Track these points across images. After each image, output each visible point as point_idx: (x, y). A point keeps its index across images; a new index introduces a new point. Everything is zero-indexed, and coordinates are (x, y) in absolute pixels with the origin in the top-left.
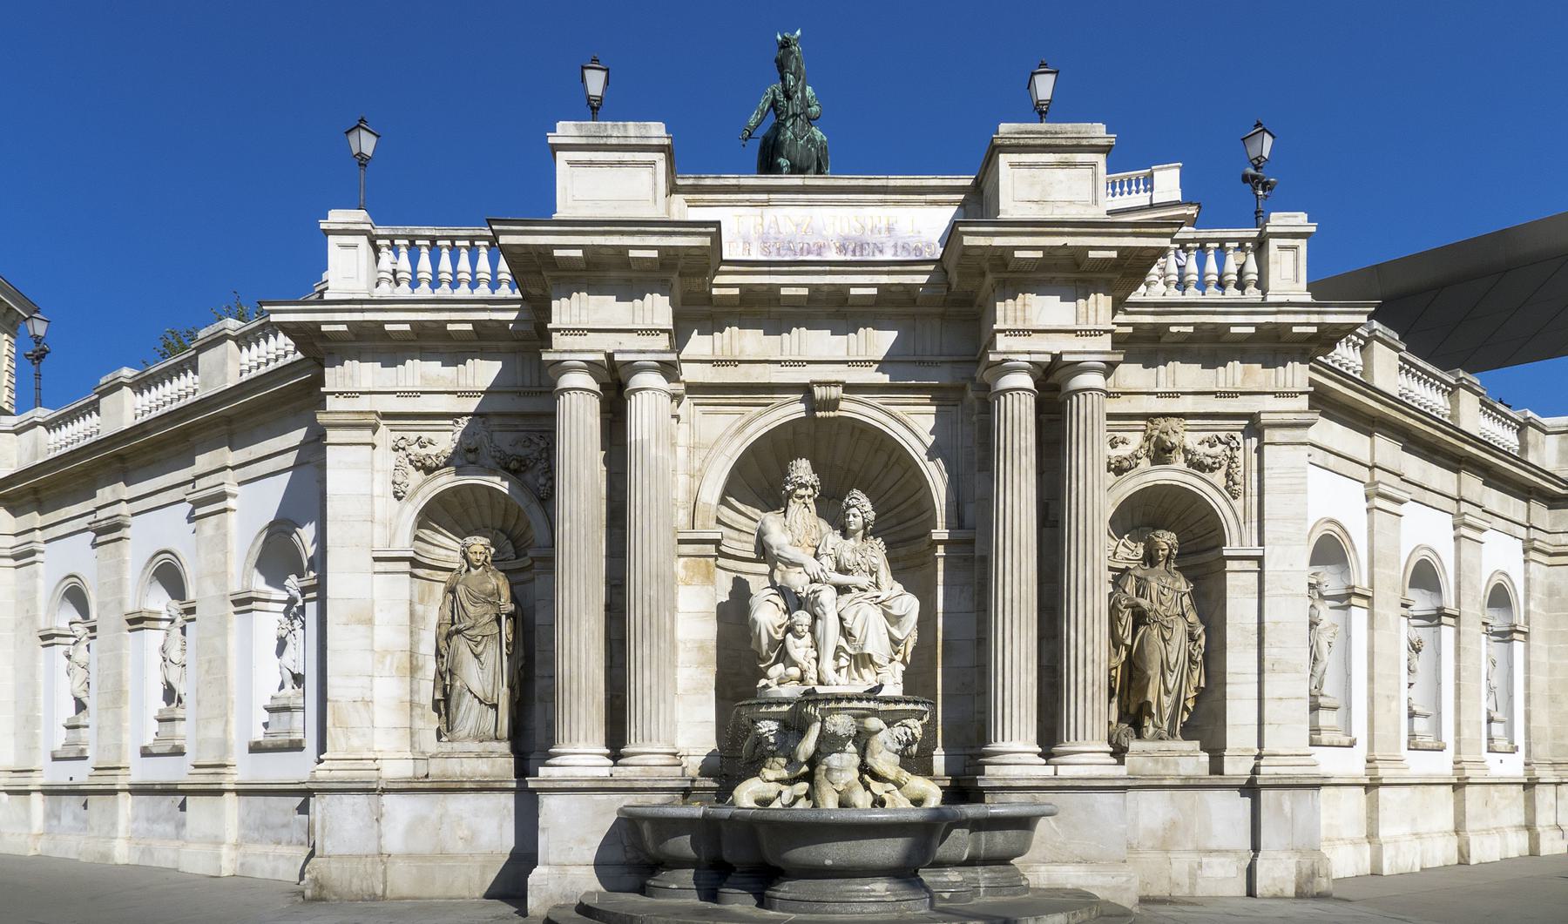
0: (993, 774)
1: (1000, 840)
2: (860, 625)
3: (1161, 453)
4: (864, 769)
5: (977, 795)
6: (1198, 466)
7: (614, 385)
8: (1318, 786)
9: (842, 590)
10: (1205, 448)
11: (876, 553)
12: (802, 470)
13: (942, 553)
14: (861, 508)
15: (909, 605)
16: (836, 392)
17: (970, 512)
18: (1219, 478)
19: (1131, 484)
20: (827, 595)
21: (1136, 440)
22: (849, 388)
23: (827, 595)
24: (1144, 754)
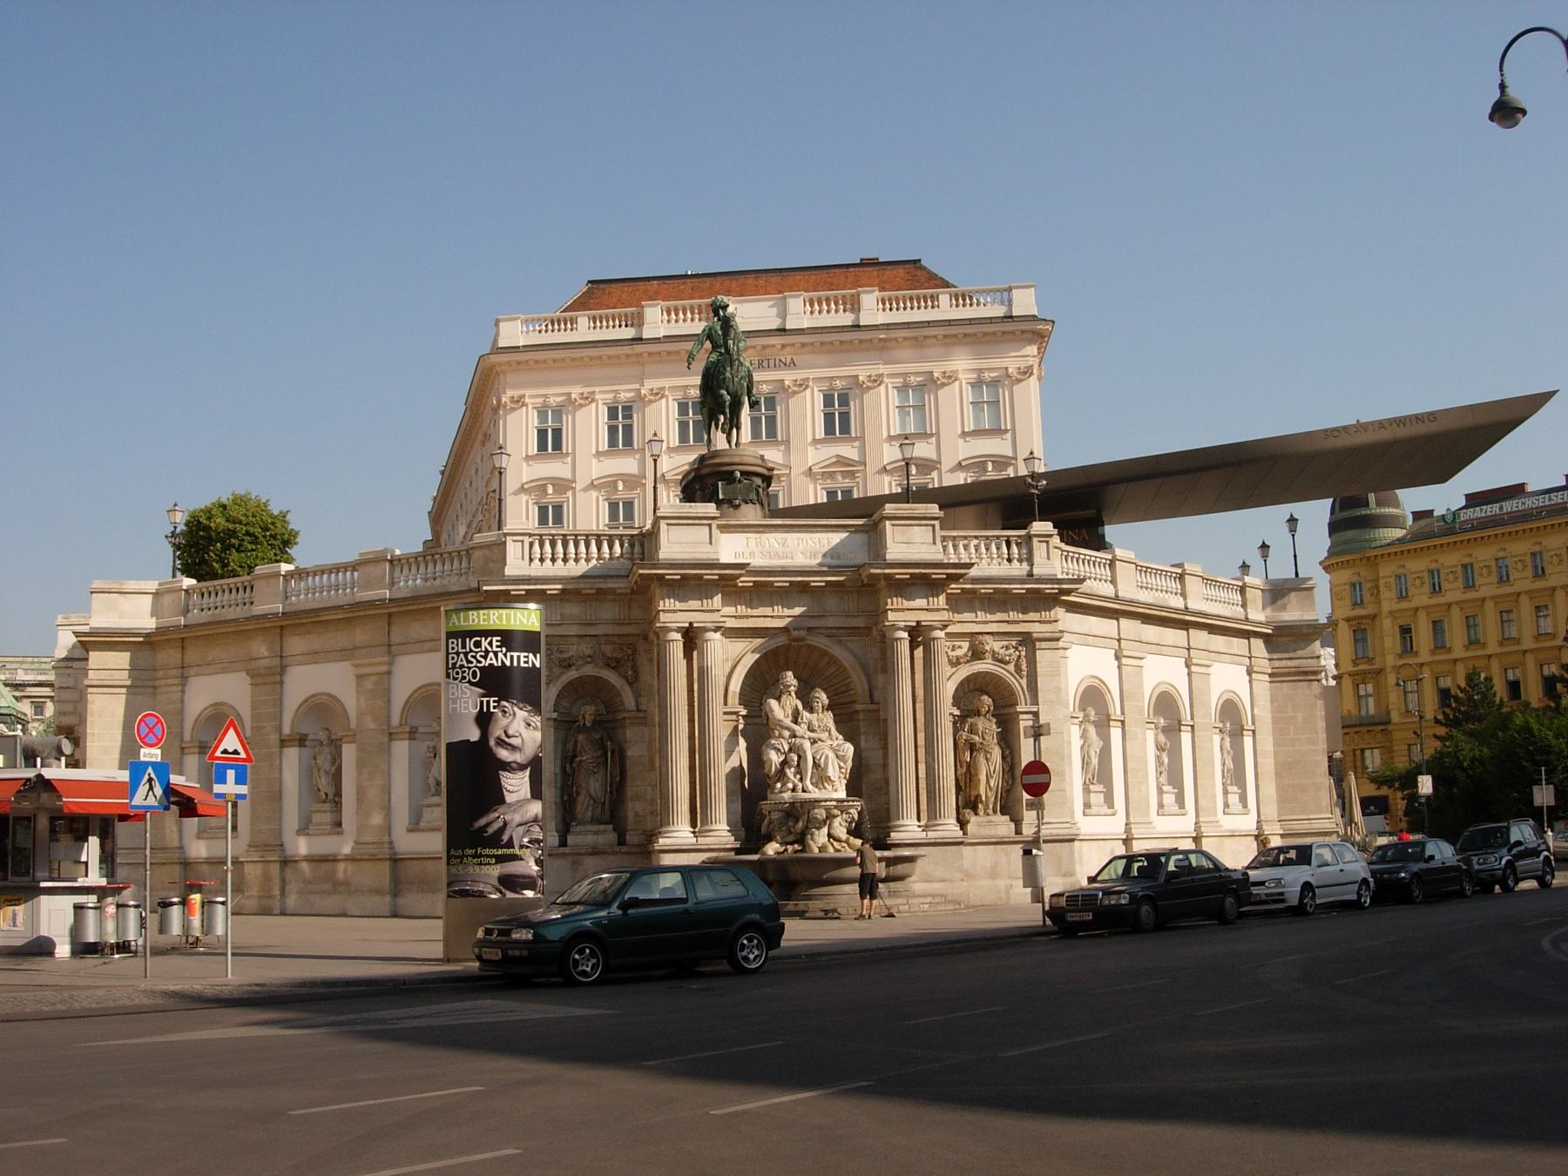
0: (895, 836)
1: (900, 869)
2: (819, 756)
3: (977, 654)
4: (830, 836)
5: (888, 847)
6: (998, 660)
7: (692, 637)
8: (1072, 840)
9: (814, 742)
10: (1002, 651)
11: (828, 719)
12: (790, 678)
13: (864, 718)
14: (822, 697)
15: (849, 749)
16: (803, 633)
17: (877, 694)
18: (1011, 667)
19: (965, 671)
20: (807, 745)
21: (966, 645)
22: (809, 629)
23: (807, 745)
24: (974, 822)
